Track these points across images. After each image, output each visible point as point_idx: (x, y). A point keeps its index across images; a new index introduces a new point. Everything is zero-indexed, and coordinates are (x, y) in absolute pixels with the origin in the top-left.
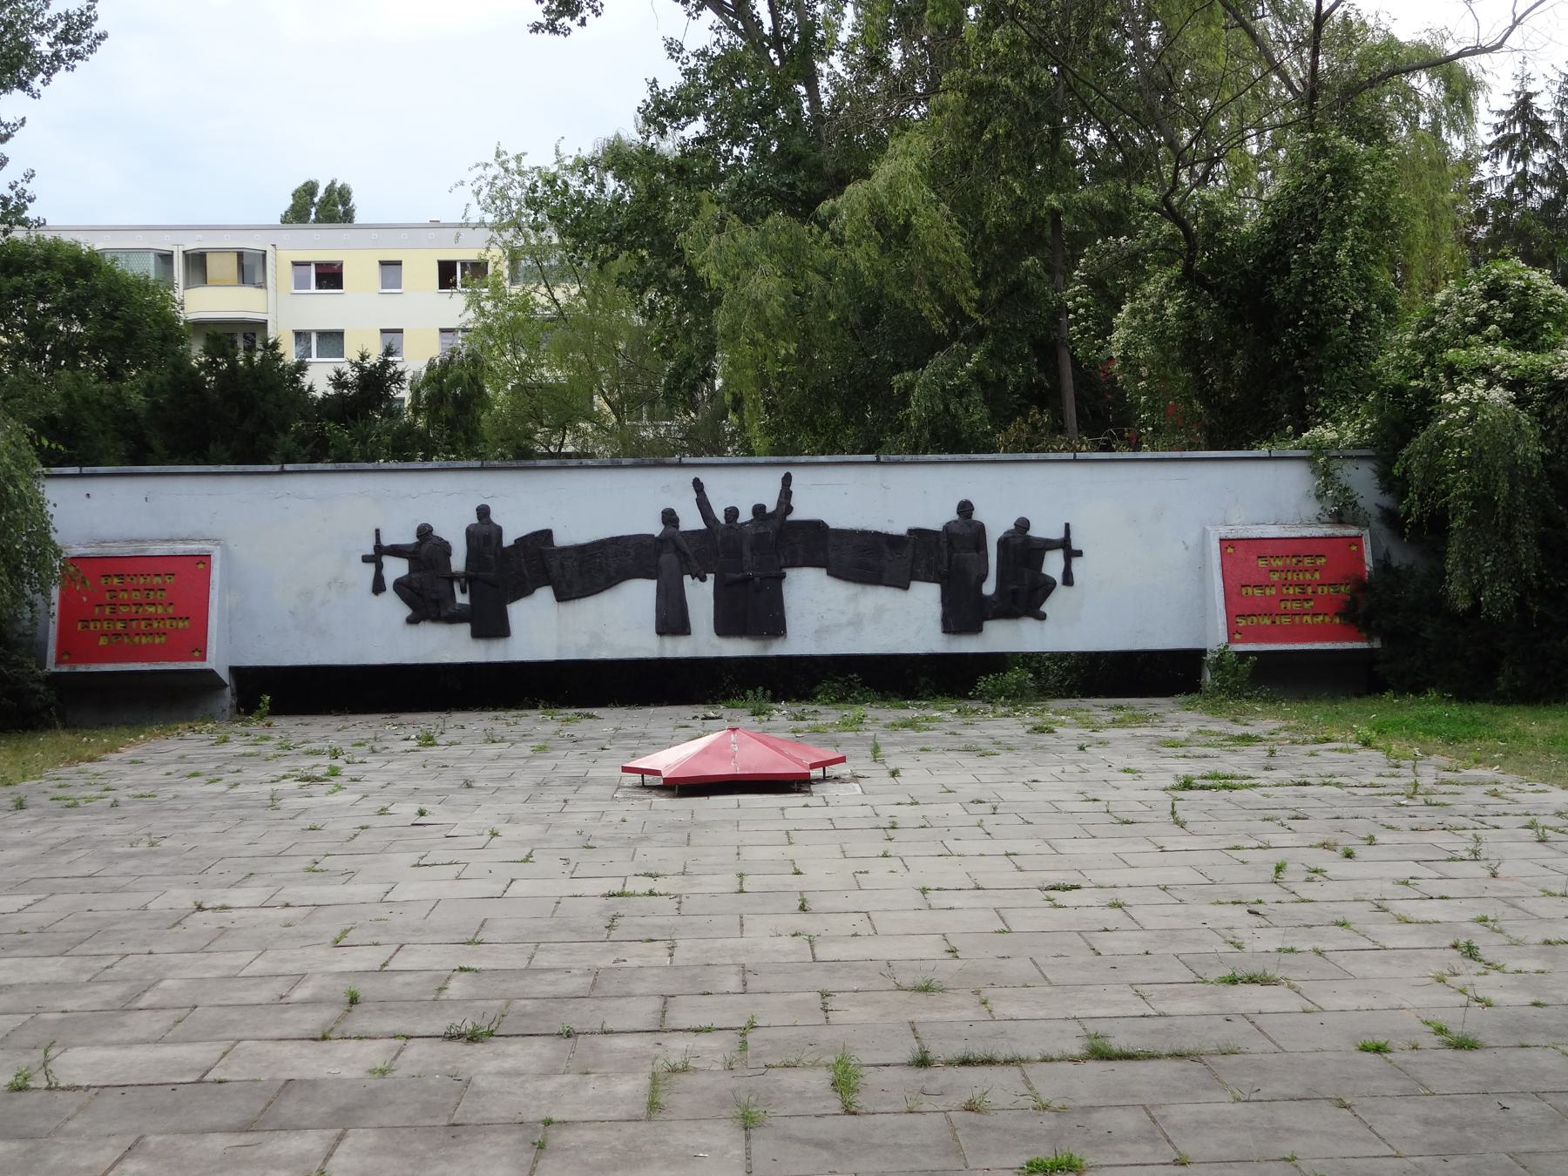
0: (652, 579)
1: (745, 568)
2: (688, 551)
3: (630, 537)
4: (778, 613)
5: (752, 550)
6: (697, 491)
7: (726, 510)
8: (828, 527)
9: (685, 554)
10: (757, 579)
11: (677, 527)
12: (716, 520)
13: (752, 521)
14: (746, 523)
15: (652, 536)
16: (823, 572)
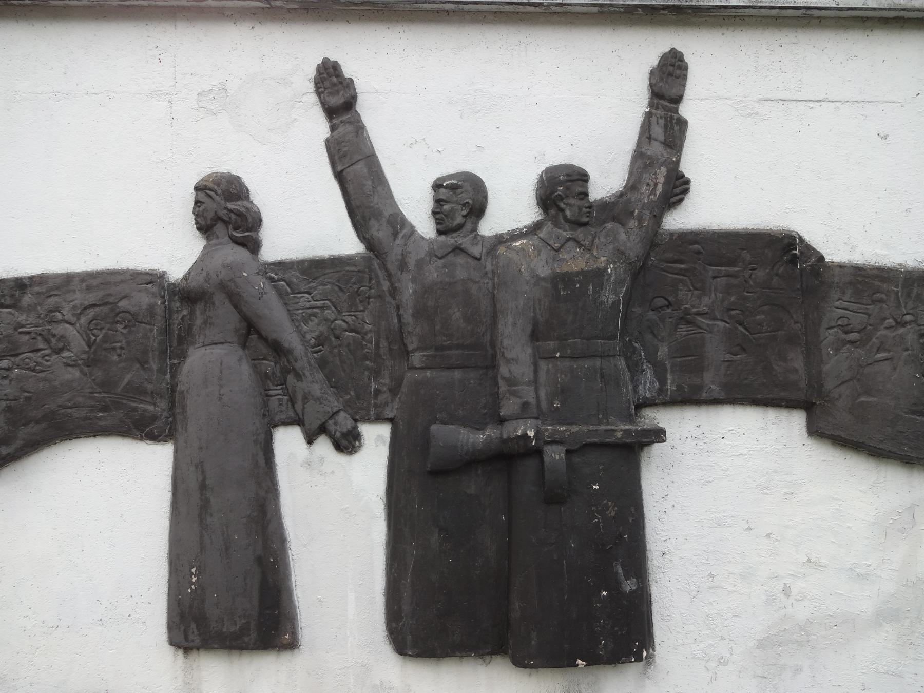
0: (154, 437)
1: (509, 407)
2: (290, 338)
3: (66, 281)
4: (629, 586)
5: (535, 336)
6: (331, 112)
7: (437, 186)
8: (821, 258)
9: (278, 349)
10: (555, 455)
11: (253, 245)
12: (398, 223)
13: (535, 228)
14: (514, 236)
15: (154, 279)
16: (796, 421)
